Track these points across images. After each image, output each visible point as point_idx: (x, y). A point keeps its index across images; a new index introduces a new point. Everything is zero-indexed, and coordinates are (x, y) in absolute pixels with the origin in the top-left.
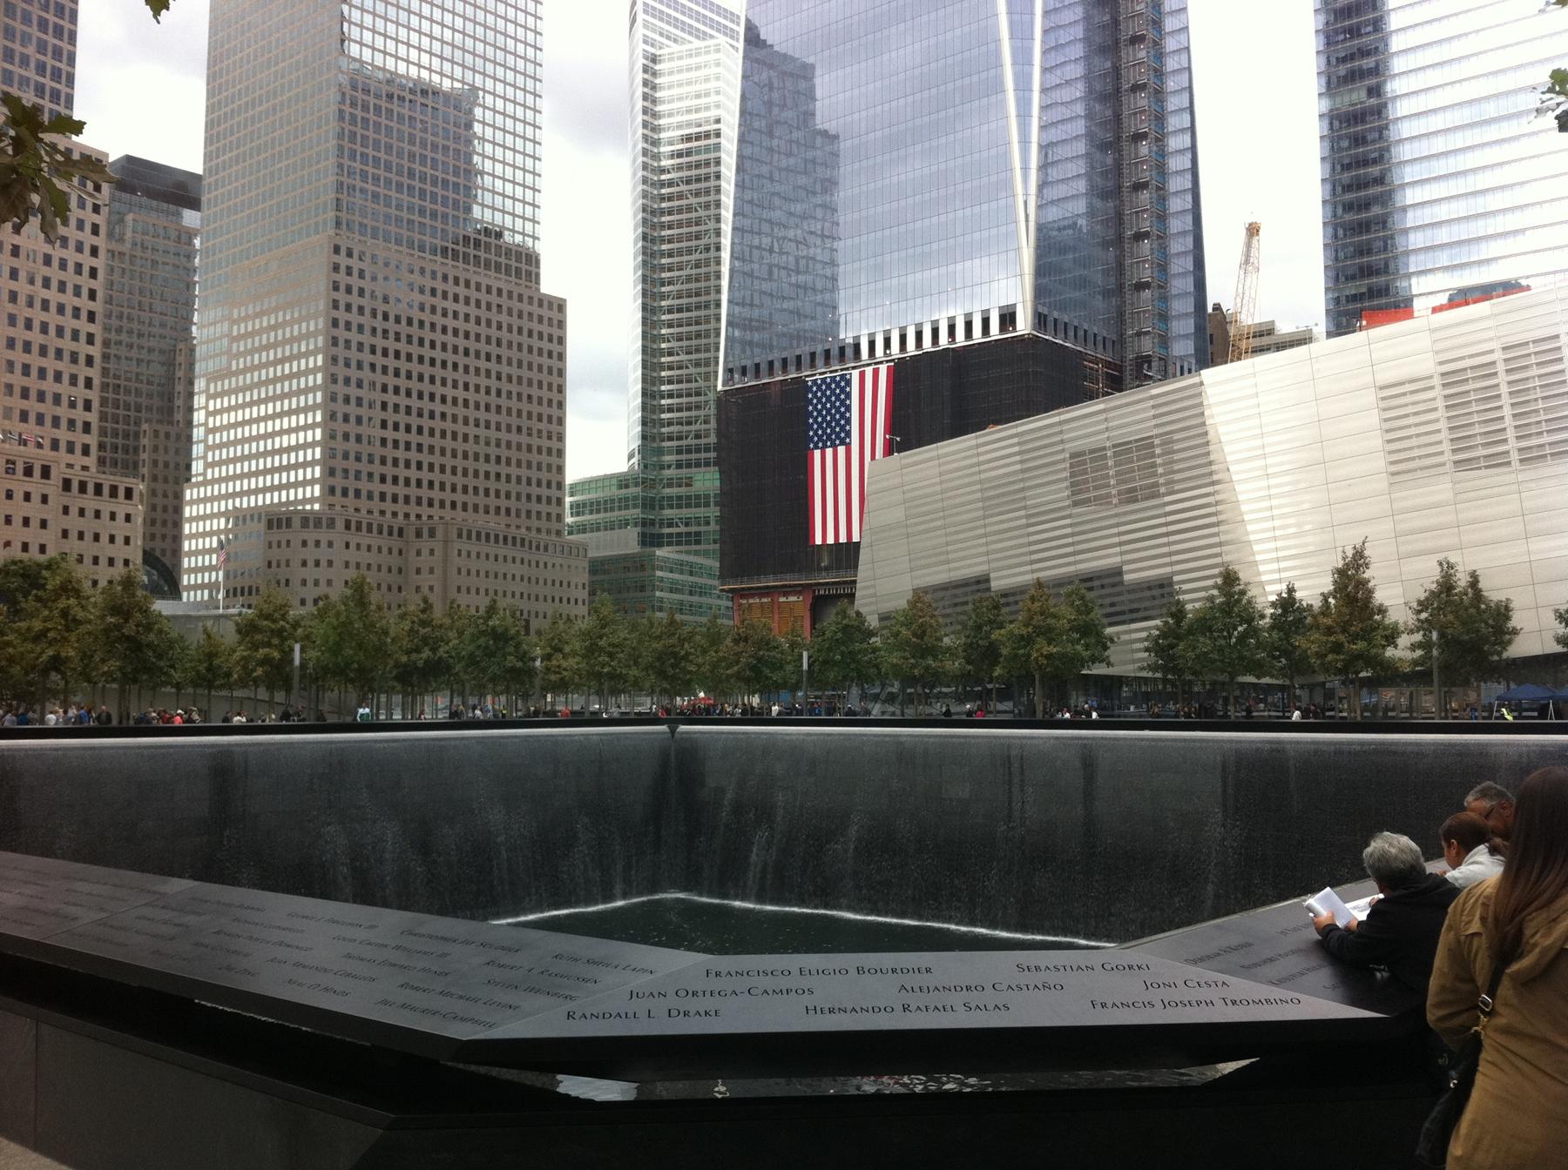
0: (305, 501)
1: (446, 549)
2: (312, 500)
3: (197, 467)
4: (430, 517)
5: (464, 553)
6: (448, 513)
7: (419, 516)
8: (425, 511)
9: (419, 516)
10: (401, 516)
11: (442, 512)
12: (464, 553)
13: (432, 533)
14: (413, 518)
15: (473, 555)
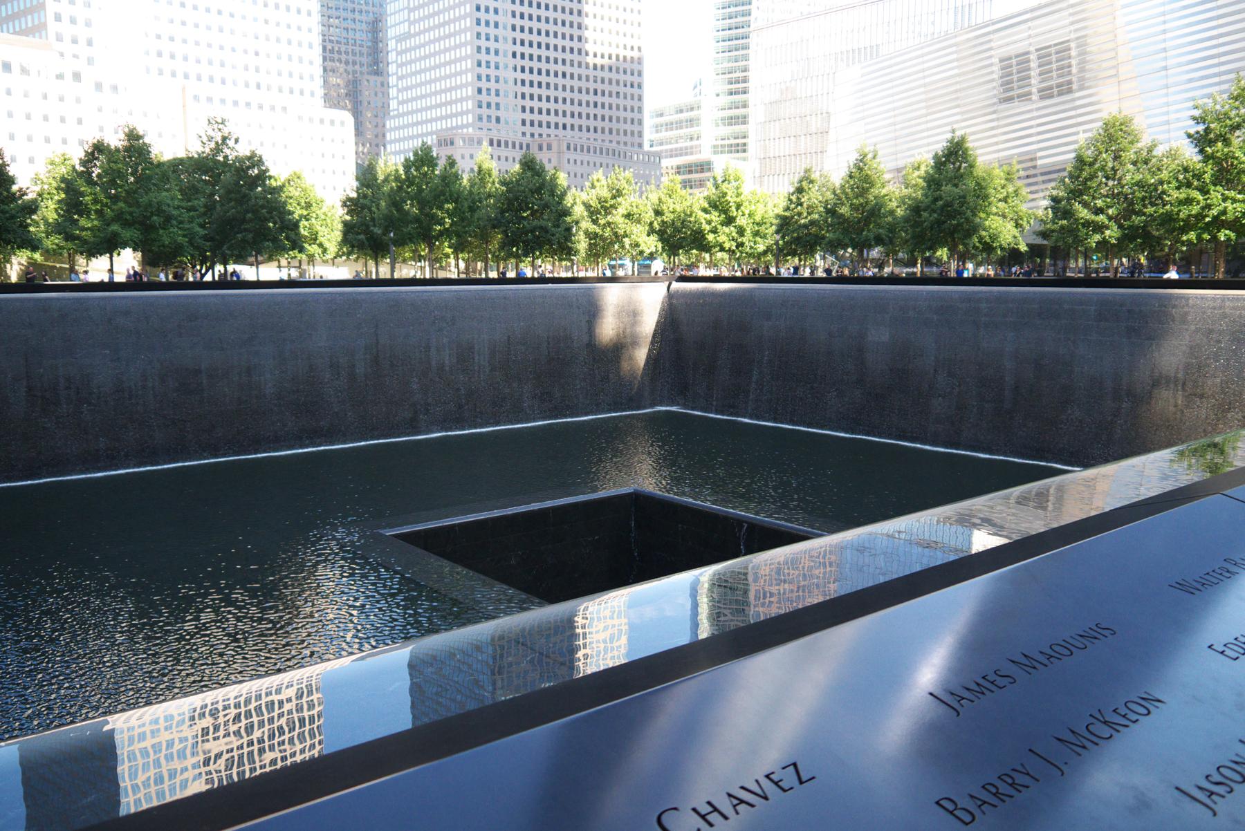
0: (463, 126)
1: (559, 157)
2: (467, 126)
3: (393, 104)
4: (549, 136)
5: (572, 161)
6: (560, 131)
7: (540, 135)
8: (544, 131)
9: (540, 135)
10: (528, 135)
11: (557, 132)
12: (572, 161)
13: (549, 148)
14: (536, 136)
15: (579, 162)
